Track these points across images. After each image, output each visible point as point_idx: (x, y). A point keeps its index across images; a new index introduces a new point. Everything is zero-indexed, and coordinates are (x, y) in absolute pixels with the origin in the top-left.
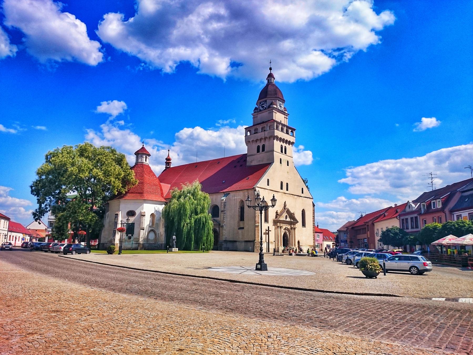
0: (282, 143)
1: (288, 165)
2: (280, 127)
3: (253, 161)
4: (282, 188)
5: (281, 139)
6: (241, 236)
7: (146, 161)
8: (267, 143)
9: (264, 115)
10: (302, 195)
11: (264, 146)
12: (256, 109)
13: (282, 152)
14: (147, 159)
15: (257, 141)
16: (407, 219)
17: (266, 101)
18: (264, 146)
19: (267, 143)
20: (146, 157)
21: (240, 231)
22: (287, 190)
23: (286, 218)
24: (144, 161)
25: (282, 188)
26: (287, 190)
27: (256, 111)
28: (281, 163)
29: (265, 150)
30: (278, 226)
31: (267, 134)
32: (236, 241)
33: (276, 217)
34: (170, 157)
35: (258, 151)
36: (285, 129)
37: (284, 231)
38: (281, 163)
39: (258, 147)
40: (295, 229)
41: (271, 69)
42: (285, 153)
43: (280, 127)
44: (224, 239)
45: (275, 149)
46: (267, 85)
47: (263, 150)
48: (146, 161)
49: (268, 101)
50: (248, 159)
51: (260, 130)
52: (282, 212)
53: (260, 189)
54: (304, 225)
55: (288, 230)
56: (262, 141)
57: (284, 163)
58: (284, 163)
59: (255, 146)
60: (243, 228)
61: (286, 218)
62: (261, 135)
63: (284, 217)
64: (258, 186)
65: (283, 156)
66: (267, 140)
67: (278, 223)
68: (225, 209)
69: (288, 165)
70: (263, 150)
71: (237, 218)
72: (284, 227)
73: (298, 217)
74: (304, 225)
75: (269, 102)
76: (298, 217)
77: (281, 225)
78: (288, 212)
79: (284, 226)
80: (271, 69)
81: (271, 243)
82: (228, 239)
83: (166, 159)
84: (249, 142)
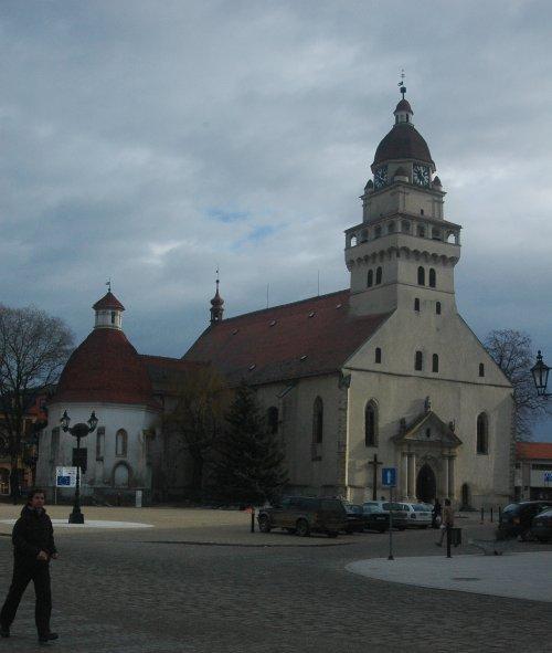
1: (438, 311)
2: (414, 227)
3: (362, 308)
4: (419, 366)
7: (113, 321)
8: (386, 266)
10: (480, 380)
11: (379, 270)
13: (421, 282)
15: (366, 258)
18: (379, 270)
19: (386, 266)
20: (114, 315)
21: (316, 465)
22: (435, 369)
23: (428, 434)
24: (110, 323)
26: (435, 369)
29: (384, 280)
34: (221, 296)
35: (370, 283)
39: (370, 272)
40: (451, 458)
41: (403, 90)
42: (433, 283)
43: (414, 227)
45: (400, 278)
46: (396, 128)
47: (379, 281)
48: (113, 321)
49: (390, 166)
50: (353, 300)
51: (372, 234)
53: (353, 373)
56: (377, 260)
57: (428, 311)
58: (428, 311)
59: (364, 270)
60: (320, 459)
61: (428, 434)
62: (370, 248)
64: (348, 364)
65: (423, 293)
66: (385, 258)
69: (438, 311)
70: (379, 281)
73: (467, 430)
74: (482, 448)
75: (392, 168)
76: (467, 430)
78: (433, 418)
80: (403, 90)
84: (352, 261)
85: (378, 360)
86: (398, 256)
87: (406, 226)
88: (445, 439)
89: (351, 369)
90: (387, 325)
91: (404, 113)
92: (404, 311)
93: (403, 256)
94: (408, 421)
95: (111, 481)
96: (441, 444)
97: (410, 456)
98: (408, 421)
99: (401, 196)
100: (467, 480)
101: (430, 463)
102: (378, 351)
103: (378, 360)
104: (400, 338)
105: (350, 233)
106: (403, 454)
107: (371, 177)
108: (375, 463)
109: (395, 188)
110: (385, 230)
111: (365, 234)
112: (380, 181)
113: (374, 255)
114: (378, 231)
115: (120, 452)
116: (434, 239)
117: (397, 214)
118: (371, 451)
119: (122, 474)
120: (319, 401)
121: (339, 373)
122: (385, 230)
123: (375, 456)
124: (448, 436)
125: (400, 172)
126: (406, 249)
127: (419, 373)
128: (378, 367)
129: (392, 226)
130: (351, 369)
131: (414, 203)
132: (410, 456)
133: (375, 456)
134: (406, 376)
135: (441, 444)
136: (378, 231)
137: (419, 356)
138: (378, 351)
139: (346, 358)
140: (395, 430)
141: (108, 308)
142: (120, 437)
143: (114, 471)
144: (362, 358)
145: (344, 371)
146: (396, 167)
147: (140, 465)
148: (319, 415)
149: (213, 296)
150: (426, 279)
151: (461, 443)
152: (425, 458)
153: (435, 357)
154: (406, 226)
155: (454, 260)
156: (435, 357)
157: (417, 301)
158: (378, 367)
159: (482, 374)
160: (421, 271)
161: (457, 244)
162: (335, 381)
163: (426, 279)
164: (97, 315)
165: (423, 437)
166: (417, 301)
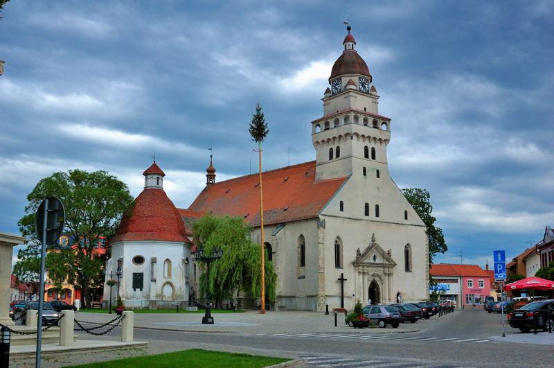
0: (367, 143)
1: (378, 176)
2: (361, 118)
4: (367, 213)
5: (363, 136)
6: (303, 288)
7: (158, 184)
9: (339, 103)
11: (338, 148)
12: (328, 91)
13: (367, 156)
14: (160, 180)
16: (546, 254)
17: (341, 79)
18: (338, 148)
22: (377, 215)
23: (375, 259)
25: (367, 213)
26: (377, 215)
27: (328, 95)
28: (365, 174)
30: (360, 272)
31: (342, 130)
32: (294, 297)
33: (357, 258)
34: (214, 166)
35: (331, 157)
36: (371, 120)
37: (372, 279)
38: (365, 174)
40: (389, 275)
41: (349, 29)
42: (374, 157)
43: (361, 118)
44: (277, 294)
45: (354, 154)
47: (338, 155)
48: (158, 184)
49: (343, 79)
51: (332, 124)
52: (369, 249)
53: (327, 219)
54: (408, 268)
55: (378, 276)
56: (336, 141)
57: (371, 175)
58: (371, 175)
60: (303, 277)
61: (375, 259)
63: (372, 257)
65: (369, 163)
66: (342, 139)
67: (359, 266)
68: (279, 249)
69: (378, 176)
71: (297, 262)
72: (371, 273)
74: (408, 268)
75: (345, 80)
77: (366, 269)
79: (372, 271)
80: (349, 29)
81: (348, 297)
82: (283, 294)
83: (208, 171)
84: (318, 142)
85: (342, 209)
86: (352, 138)
87: (356, 118)
88: (386, 262)
89: (324, 215)
90: (345, 188)
91: (351, 44)
92: (358, 174)
93: (354, 137)
94: (362, 251)
95: (161, 295)
96: (383, 266)
97: (364, 273)
98: (362, 251)
99: (352, 98)
100: (400, 290)
101: (377, 279)
102: (342, 204)
103: (342, 209)
104: (355, 194)
105: (316, 123)
106: (360, 272)
107: (330, 87)
108: (342, 280)
109: (347, 93)
110: (342, 121)
111: (327, 124)
112: (336, 88)
113: (334, 138)
114: (337, 122)
115: (166, 275)
116: (374, 127)
117: (350, 111)
118: (338, 272)
119: (168, 291)
120: (302, 236)
121: (317, 218)
122: (342, 121)
123: (342, 274)
124: (387, 260)
125: (349, 83)
126: (356, 134)
127: (367, 218)
128: (341, 214)
129: (346, 119)
130: (324, 215)
131: (359, 102)
132: (364, 273)
133: (342, 274)
134: (358, 220)
135: (383, 266)
136: (337, 122)
137: (367, 206)
138: (342, 204)
139: (321, 208)
140: (353, 257)
141: (154, 174)
142: (166, 265)
143: (162, 289)
144: (332, 208)
145: (320, 217)
146: (348, 79)
147: (179, 283)
148: (303, 248)
149: (208, 166)
150: (370, 154)
151: (395, 264)
152: (373, 275)
153: (377, 207)
154: (356, 118)
155: (387, 141)
156: (377, 207)
157: (364, 170)
158: (341, 214)
159: (406, 218)
160: (366, 149)
161: (388, 131)
162: (314, 224)
163: (370, 154)
164: (146, 179)
165: (372, 261)
166: (364, 170)
